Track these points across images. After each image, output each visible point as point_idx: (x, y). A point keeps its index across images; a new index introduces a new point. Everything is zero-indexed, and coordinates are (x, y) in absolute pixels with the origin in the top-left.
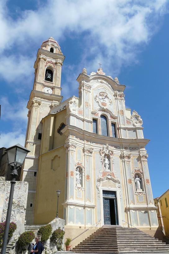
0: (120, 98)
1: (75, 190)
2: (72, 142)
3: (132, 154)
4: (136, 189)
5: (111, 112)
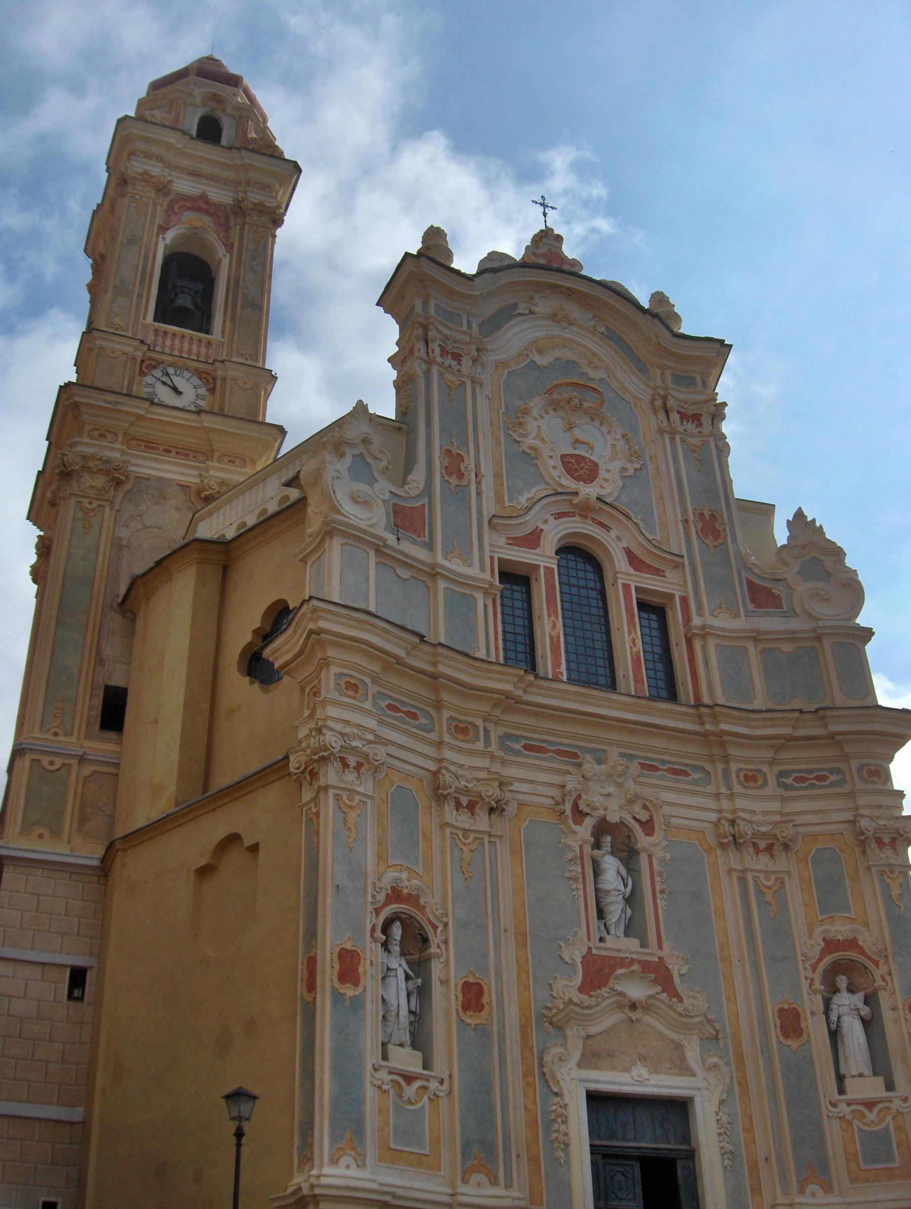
1: (370, 1093)
2: (348, 730)
4: (840, 1079)
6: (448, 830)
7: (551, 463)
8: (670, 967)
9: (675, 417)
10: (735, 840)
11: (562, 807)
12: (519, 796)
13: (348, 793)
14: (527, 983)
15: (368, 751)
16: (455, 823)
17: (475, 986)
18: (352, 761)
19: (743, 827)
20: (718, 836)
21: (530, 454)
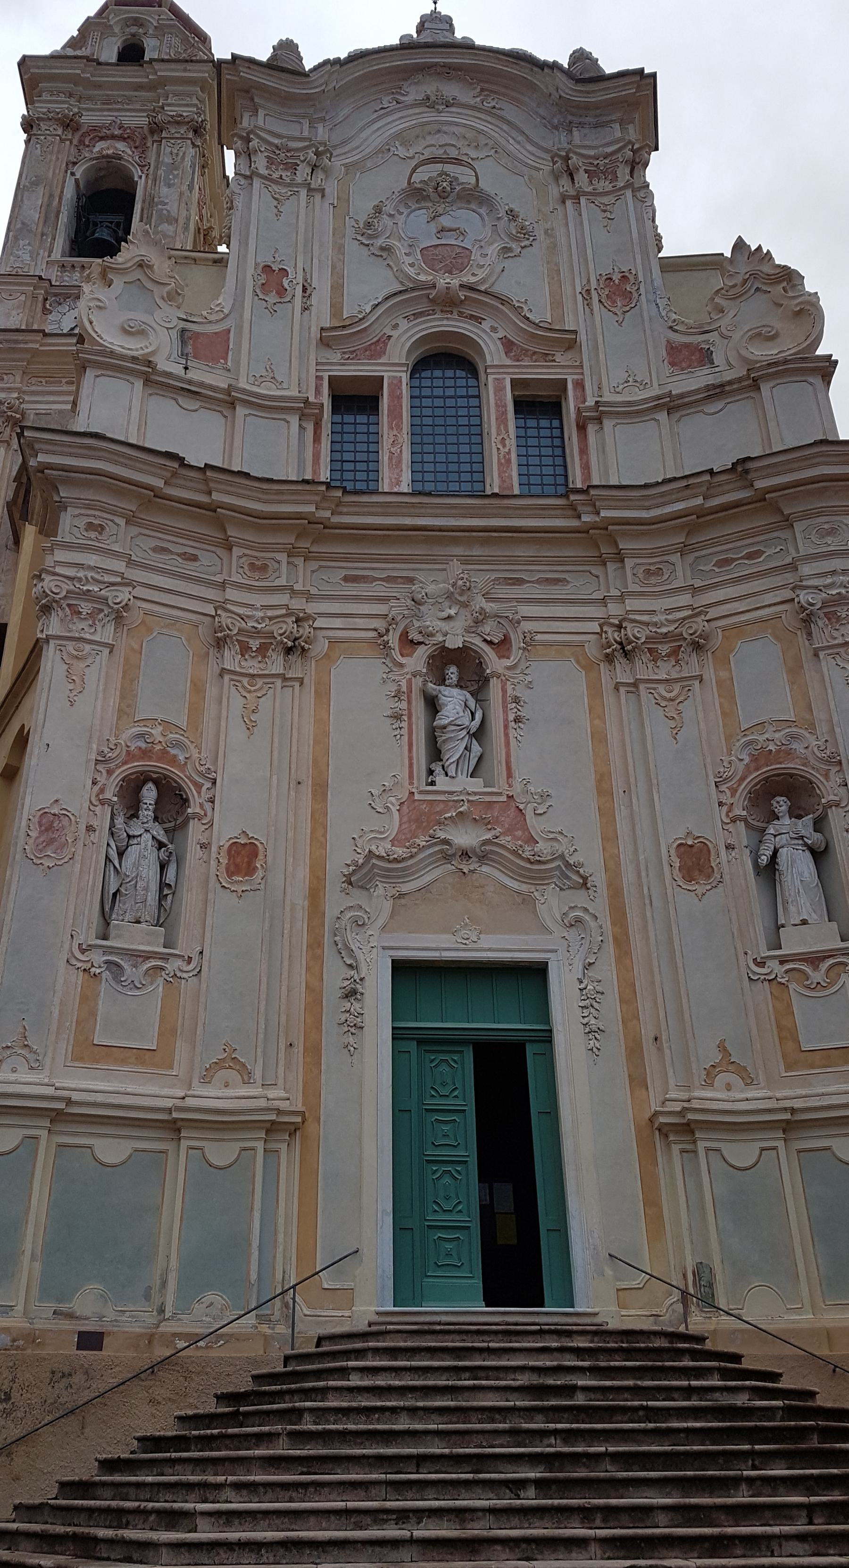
0: (603, 185)
2: (81, 574)
3: (712, 613)
5: (517, 310)
6: (227, 678)
7: (409, 260)
8: (521, 807)
9: (582, 178)
10: (623, 648)
11: (385, 638)
12: (330, 633)
13: (74, 643)
14: (322, 839)
15: (108, 594)
16: (238, 669)
17: (248, 847)
18: (86, 608)
19: (631, 630)
20: (603, 647)
21: (381, 256)
